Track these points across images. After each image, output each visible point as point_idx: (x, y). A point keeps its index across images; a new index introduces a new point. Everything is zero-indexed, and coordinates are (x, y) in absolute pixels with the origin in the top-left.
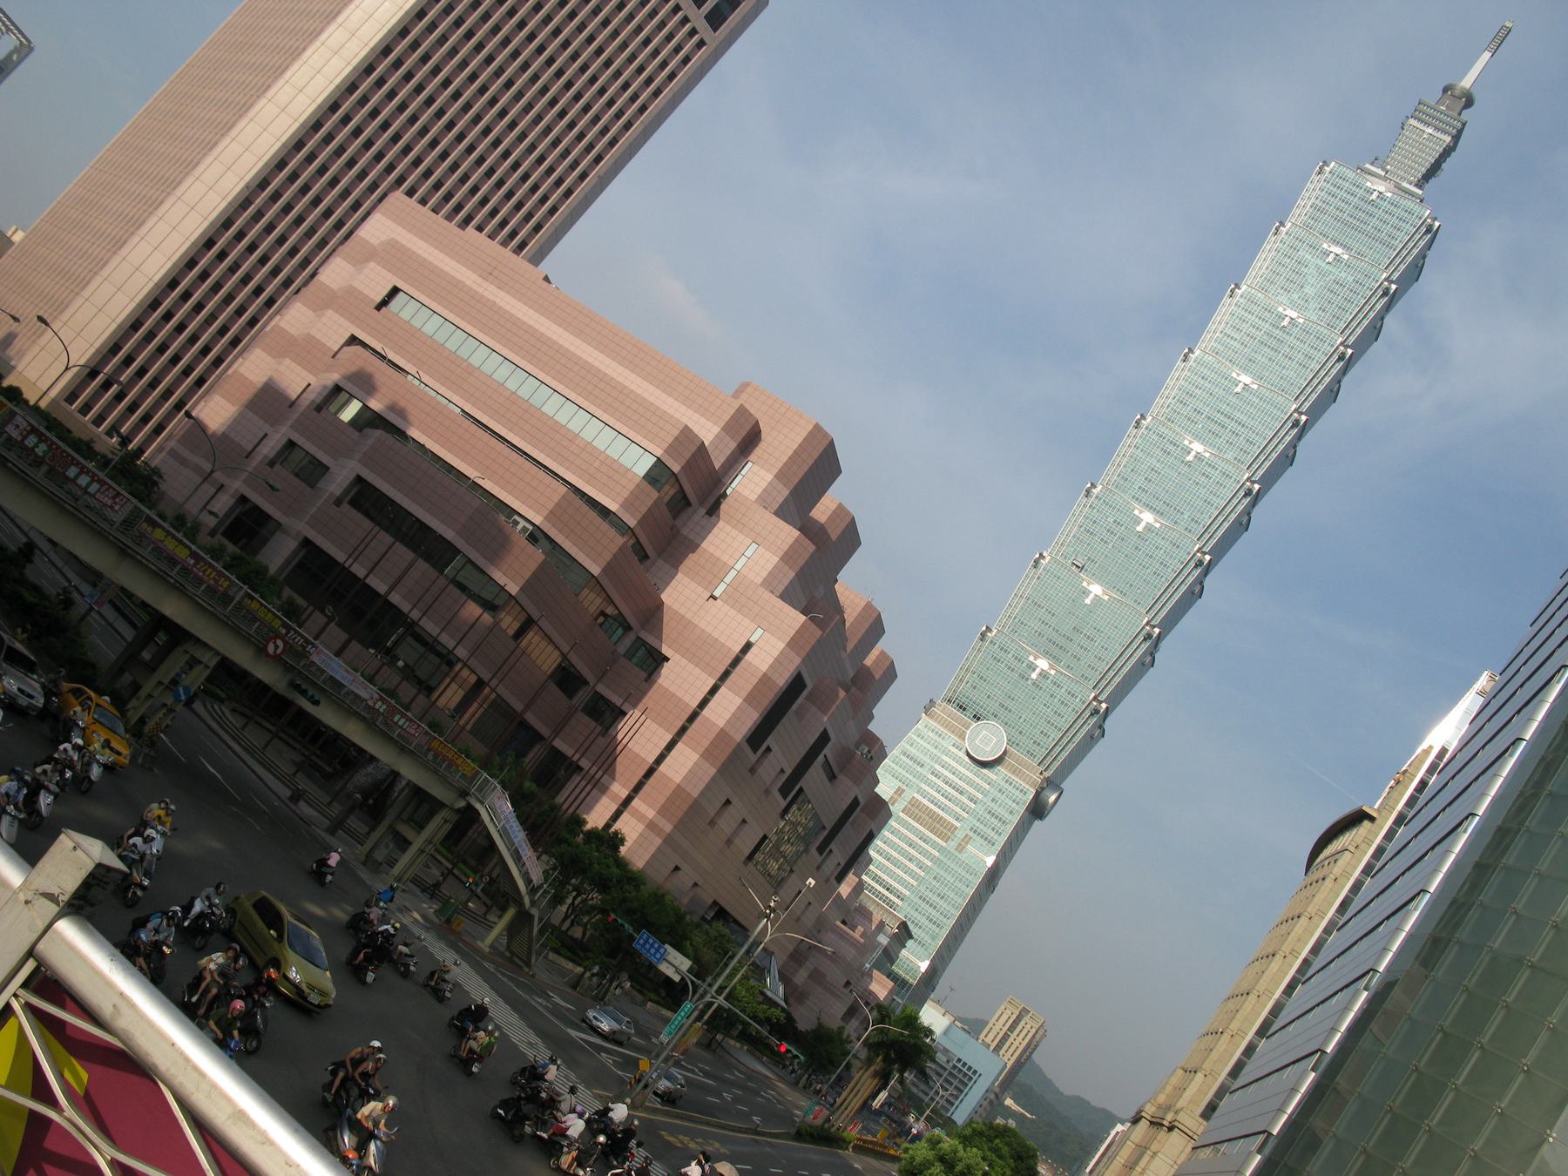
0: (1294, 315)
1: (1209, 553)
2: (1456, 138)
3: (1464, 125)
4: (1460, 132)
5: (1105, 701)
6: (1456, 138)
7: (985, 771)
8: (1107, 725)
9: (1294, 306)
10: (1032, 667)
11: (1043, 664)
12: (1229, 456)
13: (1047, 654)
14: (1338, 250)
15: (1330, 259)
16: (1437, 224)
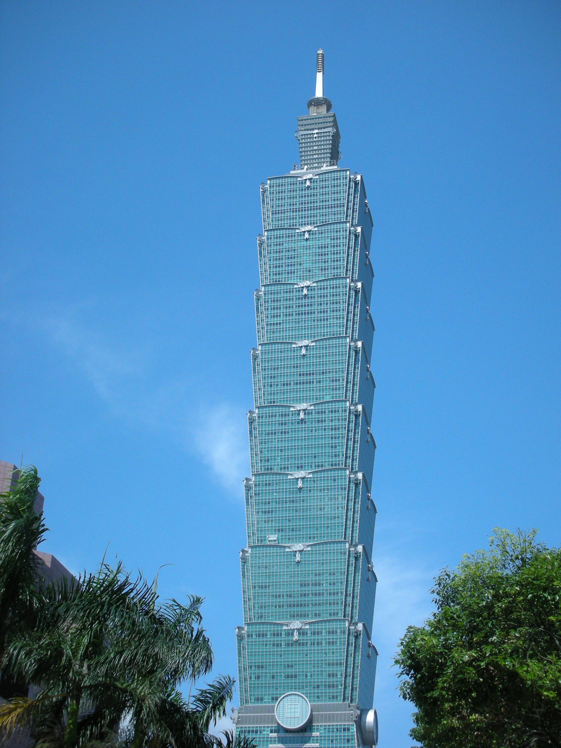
0: (307, 283)
1: (359, 471)
2: (335, 124)
3: (334, 116)
4: (335, 121)
5: (360, 620)
6: (335, 124)
7: (306, 734)
8: (374, 641)
9: (303, 278)
10: (290, 633)
11: (296, 624)
12: (328, 398)
13: (294, 616)
14: (309, 228)
15: (307, 236)
16: (359, 178)
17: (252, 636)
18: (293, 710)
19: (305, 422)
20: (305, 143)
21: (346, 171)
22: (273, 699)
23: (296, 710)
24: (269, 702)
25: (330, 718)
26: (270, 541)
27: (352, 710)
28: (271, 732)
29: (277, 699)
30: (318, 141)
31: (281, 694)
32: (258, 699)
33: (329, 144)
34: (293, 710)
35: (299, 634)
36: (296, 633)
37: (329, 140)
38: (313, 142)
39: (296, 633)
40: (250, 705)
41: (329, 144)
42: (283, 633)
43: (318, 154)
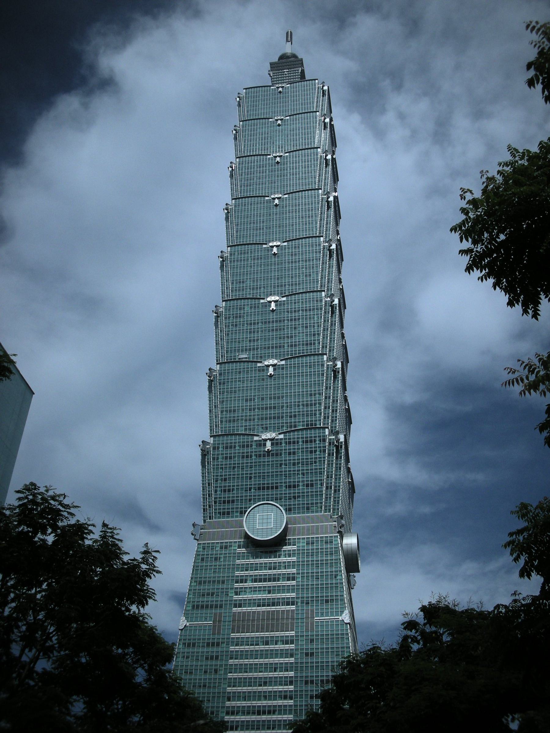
17: (218, 448)
18: (265, 521)
19: (278, 257)
20: (276, 78)
21: (315, 80)
22: (241, 513)
23: (269, 521)
24: (237, 517)
25: (309, 531)
26: (239, 359)
27: (335, 521)
28: (239, 547)
29: (245, 512)
30: (288, 77)
31: (249, 507)
32: (224, 513)
33: (298, 78)
34: (265, 521)
35: (272, 444)
36: (269, 444)
37: (298, 75)
38: (283, 77)
39: (269, 444)
40: (214, 520)
41: (298, 78)
42: (254, 444)
43: (288, 79)
